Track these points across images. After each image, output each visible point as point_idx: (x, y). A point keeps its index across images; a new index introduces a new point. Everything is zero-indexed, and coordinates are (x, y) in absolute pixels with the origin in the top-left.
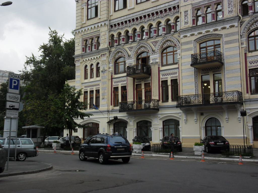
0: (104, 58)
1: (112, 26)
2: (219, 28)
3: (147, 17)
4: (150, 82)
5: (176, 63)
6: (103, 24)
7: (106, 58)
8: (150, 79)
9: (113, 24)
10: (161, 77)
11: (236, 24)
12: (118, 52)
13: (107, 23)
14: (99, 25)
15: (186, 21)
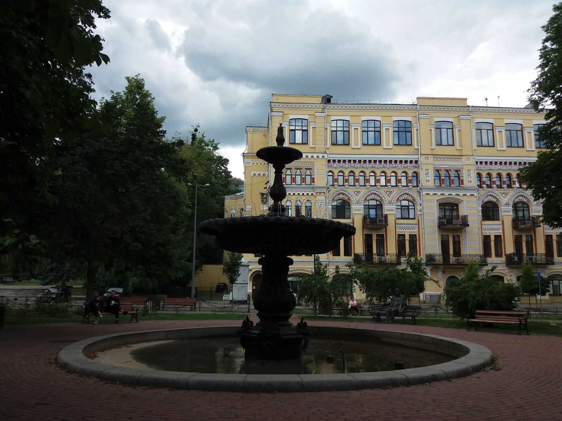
0: (321, 198)
1: (329, 161)
2: (461, 194)
3: (378, 162)
4: (385, 234)
5: (414, 219)
6: (321, 156)
7: (324, 198)
8: (384, 230)
9: (331, 159)
10: (398, 230)
11: (476, 194)
12: (339, 194)
13: (326, 156)
14: (315, 156)
15: (427, 179)
